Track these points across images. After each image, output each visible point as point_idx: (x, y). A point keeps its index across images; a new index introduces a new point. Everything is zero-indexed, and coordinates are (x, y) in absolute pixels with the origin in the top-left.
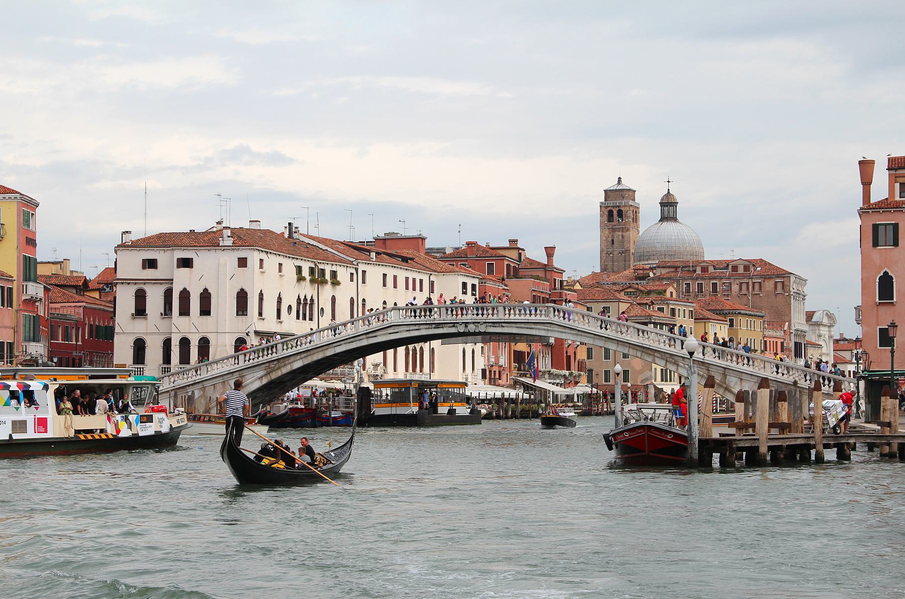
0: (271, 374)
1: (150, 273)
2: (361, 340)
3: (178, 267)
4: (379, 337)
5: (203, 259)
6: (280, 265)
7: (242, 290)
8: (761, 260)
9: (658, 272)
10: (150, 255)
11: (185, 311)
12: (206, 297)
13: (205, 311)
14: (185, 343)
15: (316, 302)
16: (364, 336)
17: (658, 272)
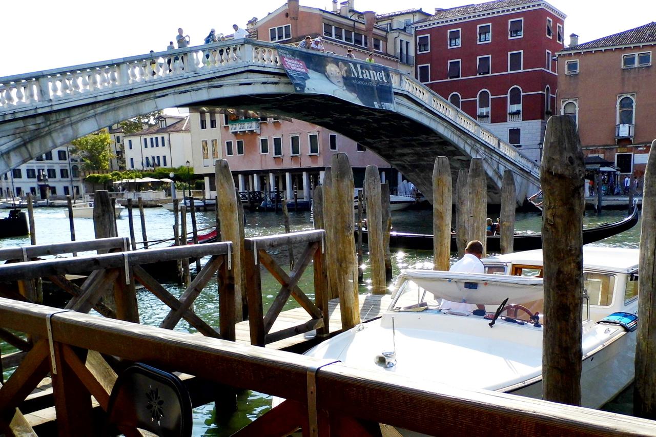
0: (29, 146)
2: (200, 89)
4: (224, 88)
16: (206, 84)
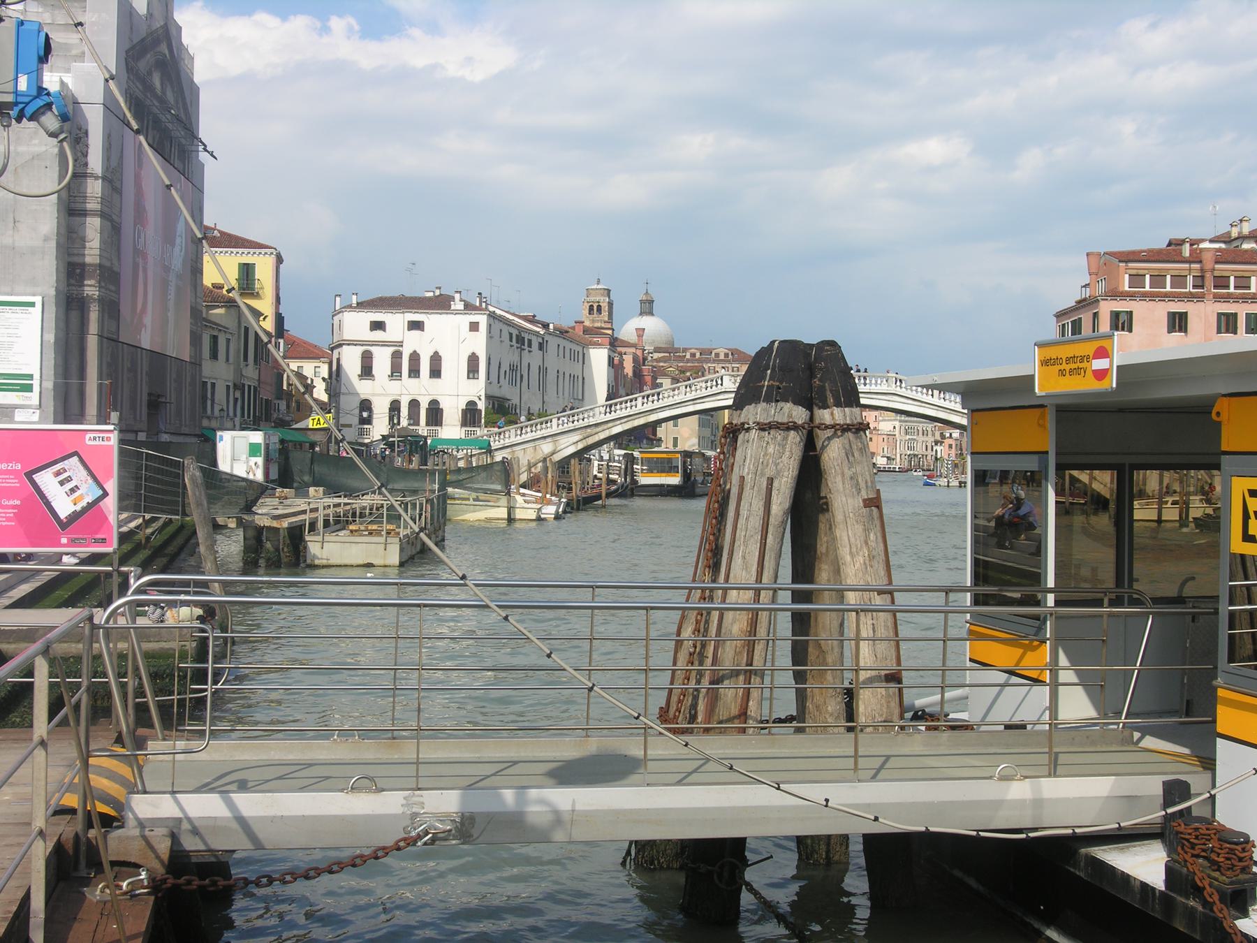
1: (378, 335)
3: (409, 330)
5: (432, 320)
6: (501, 330)
7: (473, 354)
8: (737, 350)
9: (656, 356)
11: (414, 372)
12: (436, 360)
13: (436, 373)
14: (414, 404)
15: (519, 368)
17: (656, 356)
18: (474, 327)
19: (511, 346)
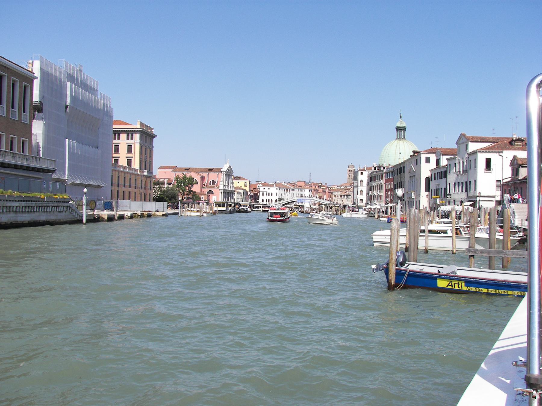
1: (264, 190)
10: (264, 188)
11: (269, 195)
13: (272, 195)
14: (269, 200)
18: (277, 189)
19: (284, 191)
